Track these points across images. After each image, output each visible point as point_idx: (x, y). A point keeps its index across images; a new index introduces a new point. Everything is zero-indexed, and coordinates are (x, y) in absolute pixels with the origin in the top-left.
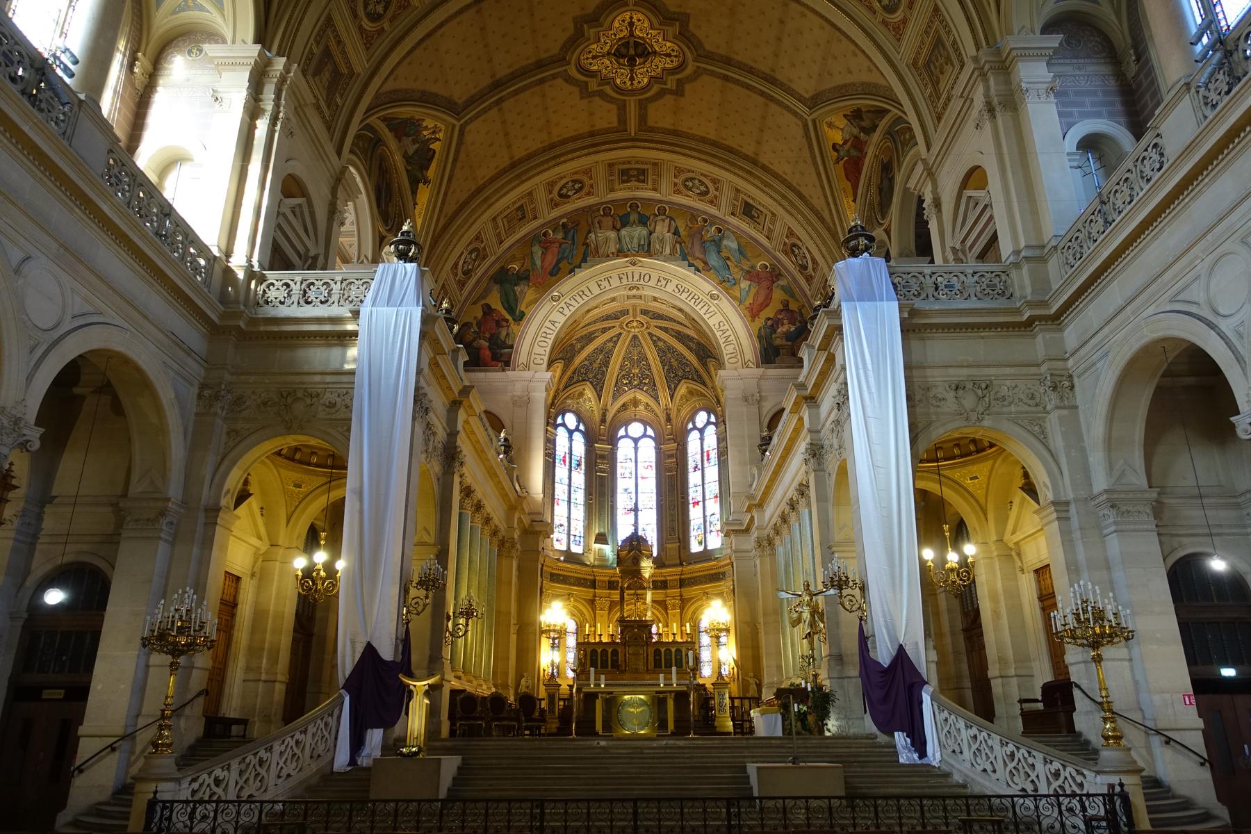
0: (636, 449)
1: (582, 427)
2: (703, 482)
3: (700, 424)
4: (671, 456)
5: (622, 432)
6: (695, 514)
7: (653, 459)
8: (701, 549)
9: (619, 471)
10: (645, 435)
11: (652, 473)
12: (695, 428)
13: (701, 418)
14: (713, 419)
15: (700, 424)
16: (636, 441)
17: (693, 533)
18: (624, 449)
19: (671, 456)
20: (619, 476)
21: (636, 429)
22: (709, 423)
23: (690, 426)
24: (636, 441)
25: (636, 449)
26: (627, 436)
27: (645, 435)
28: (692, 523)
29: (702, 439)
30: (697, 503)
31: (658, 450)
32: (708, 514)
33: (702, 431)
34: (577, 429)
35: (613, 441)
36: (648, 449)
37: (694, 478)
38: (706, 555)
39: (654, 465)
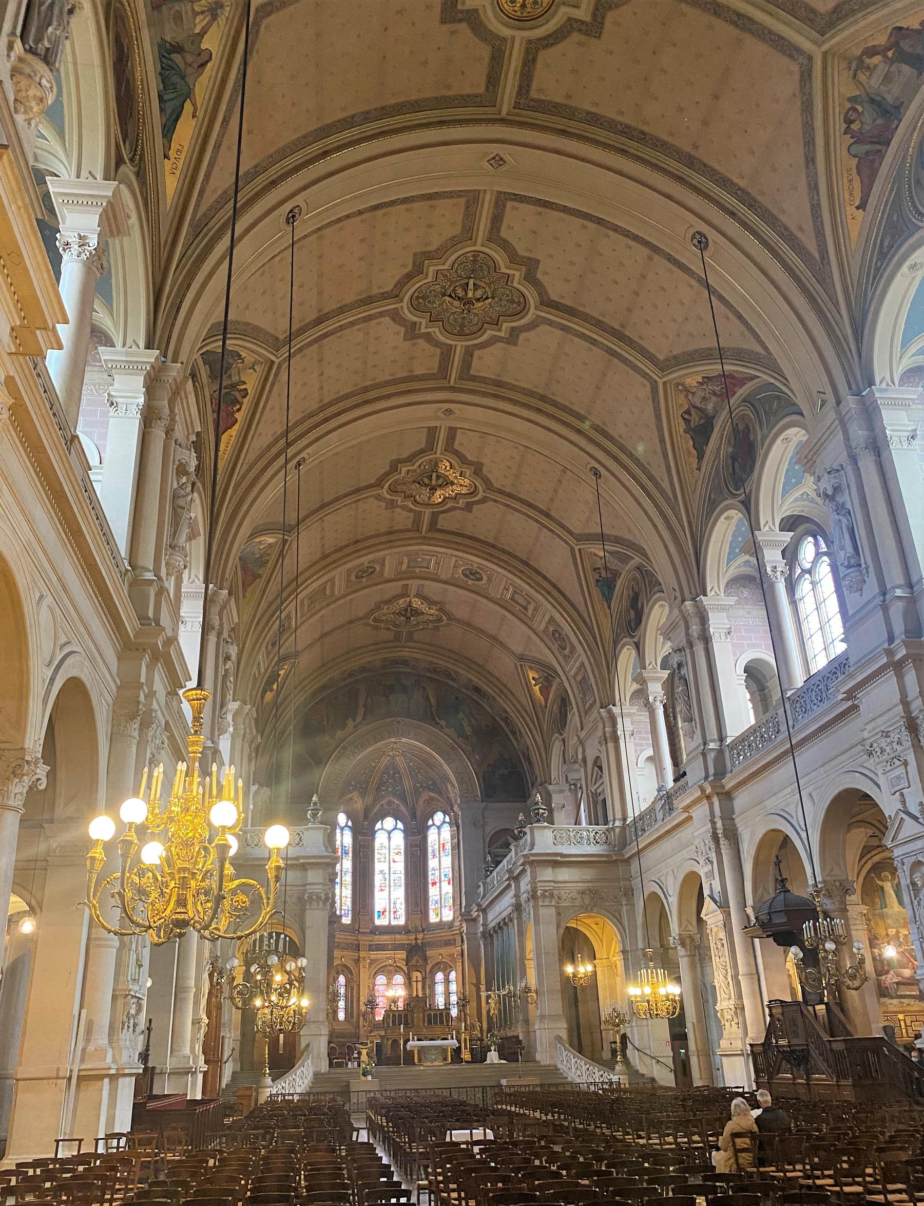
0: (389, 838)
1: (350, 824)
2: (441, 865)
3: (438, 823)
4: (416, 846)
5: (378, 826)
6: (433, 892)
7: (402, 847)
8: (438, 920)
9: (377, 856)
10: (395, 828)
11: (401, 859)
12: (434, 824)
13: (439, 817)
14: (447, 819)
15: (438, 823)
16: (389, 833)
17: (432, 906)
18: (380, 839)
19: (416, 846)
20: (376, 860)
21: (389, 822)
22: (444, 822)
23: (430, 822)
24: (389, 833)
25: (389, 838)
26: (382, 829)
27: (395, 828)
28: (431, 899)
29: (439, 834)
30: (434, 884)
31: (406, 838)
32: (443, 892)
33: (439, 828)
34: (346, 826)
35: (373, 833)
36: (399, 839)
37: (432, 863)
38: (441, 925)
39: (402, 851)
